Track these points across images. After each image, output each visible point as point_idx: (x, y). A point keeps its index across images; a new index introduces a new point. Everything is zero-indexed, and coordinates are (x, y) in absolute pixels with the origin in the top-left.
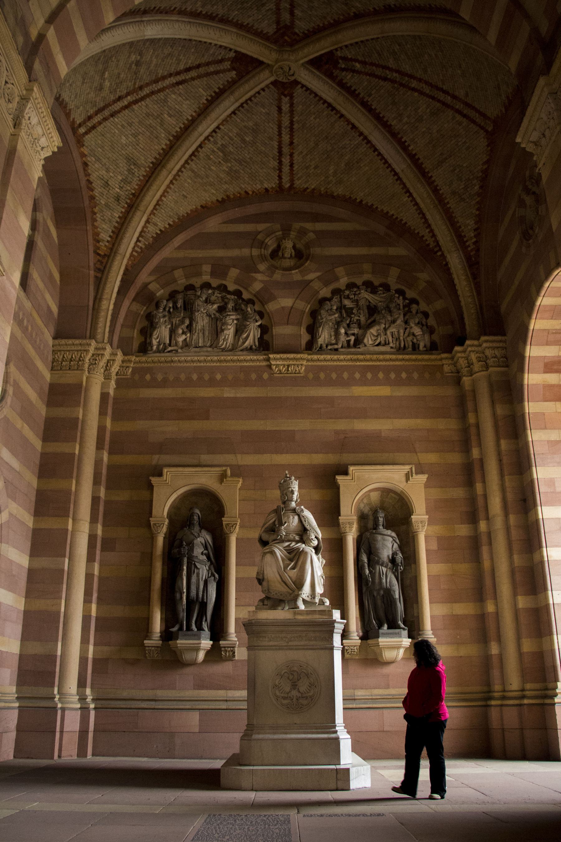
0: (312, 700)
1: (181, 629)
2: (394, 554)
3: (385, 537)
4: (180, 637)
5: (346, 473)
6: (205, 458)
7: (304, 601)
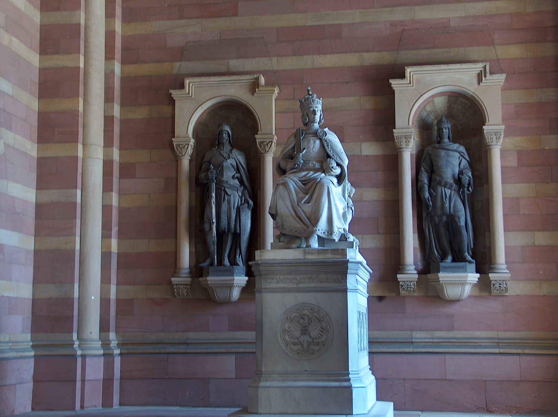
0: (324, 345)
1: (212, 264)
2: (461, 173)
3: (450, 152)
4: (210, 274)
5: (402, 76)
6: (235, 64)
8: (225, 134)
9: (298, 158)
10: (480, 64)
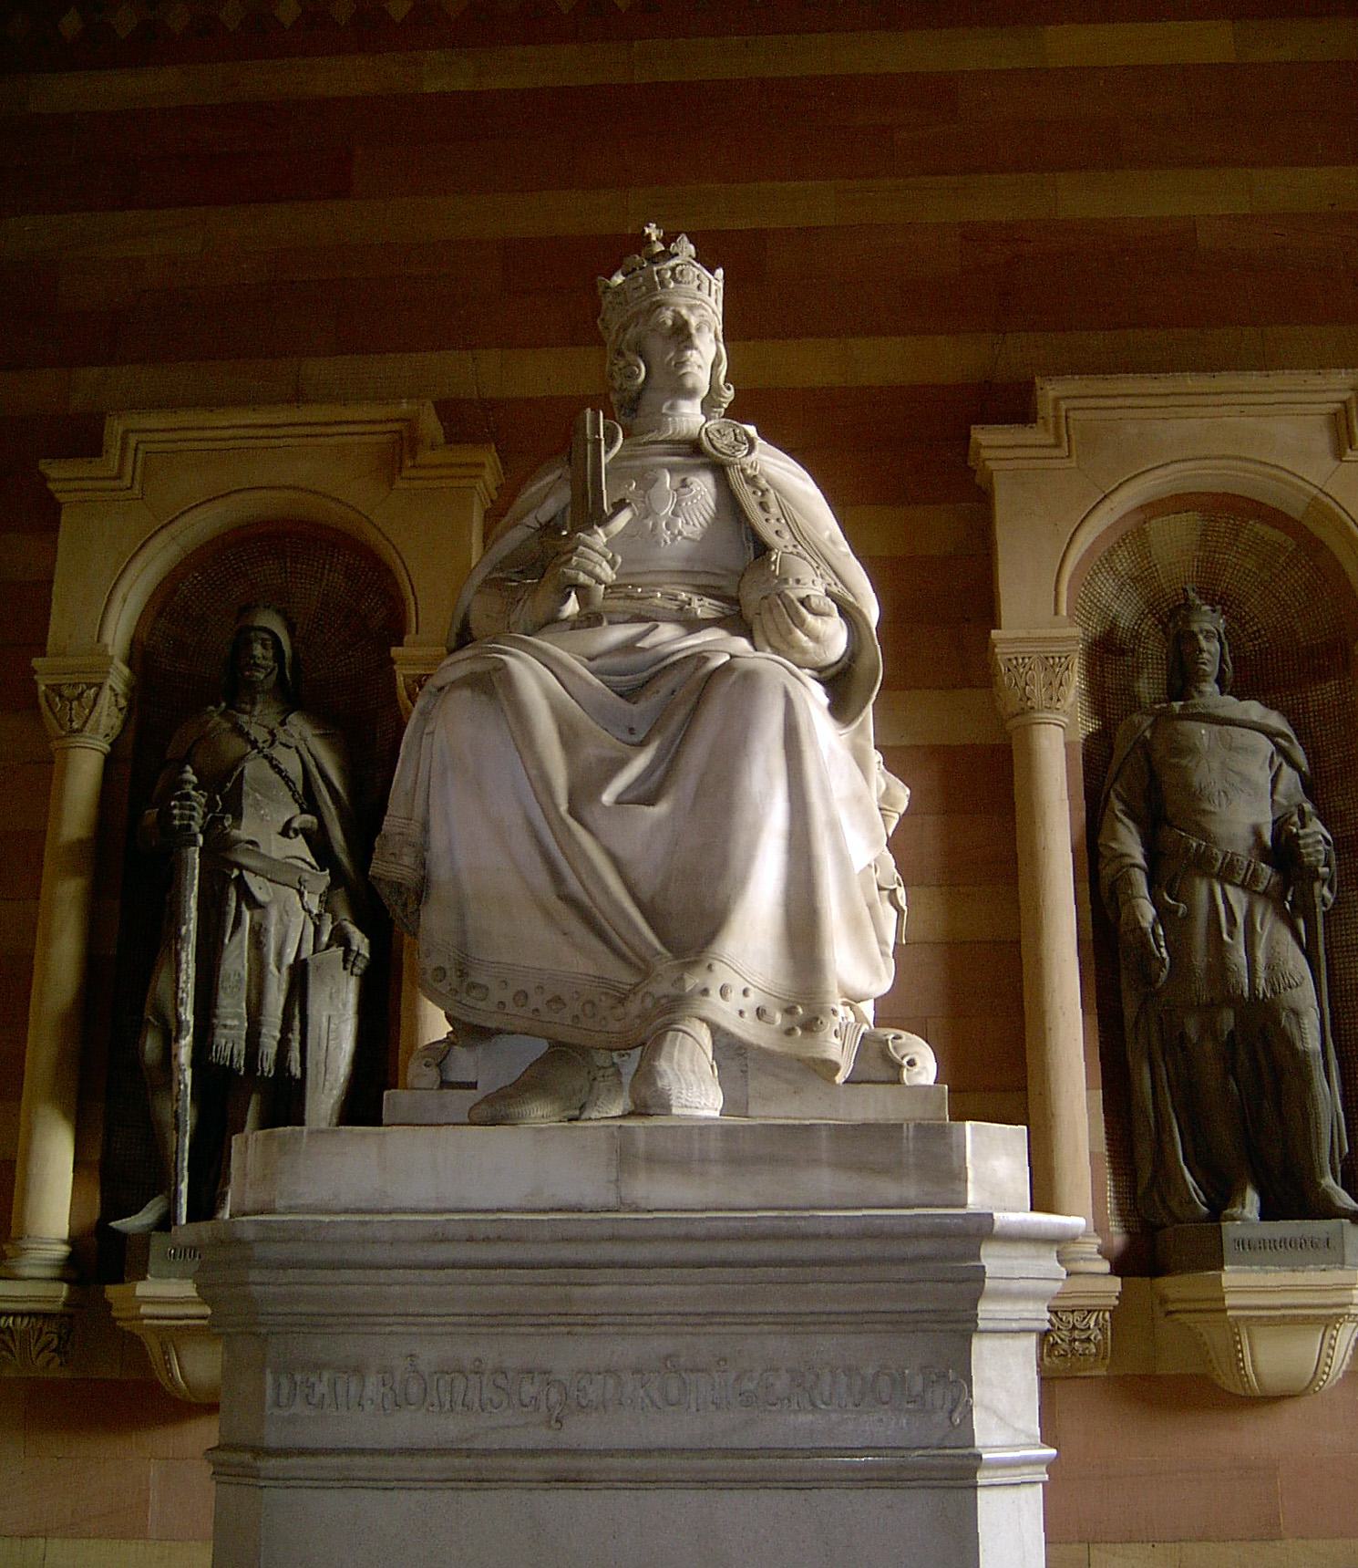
1: (166, 1222)
4: (152, 1267)
7: (730, 1051)
8: (264, 646)
9: (581, 548)
10: (1340, 373)
